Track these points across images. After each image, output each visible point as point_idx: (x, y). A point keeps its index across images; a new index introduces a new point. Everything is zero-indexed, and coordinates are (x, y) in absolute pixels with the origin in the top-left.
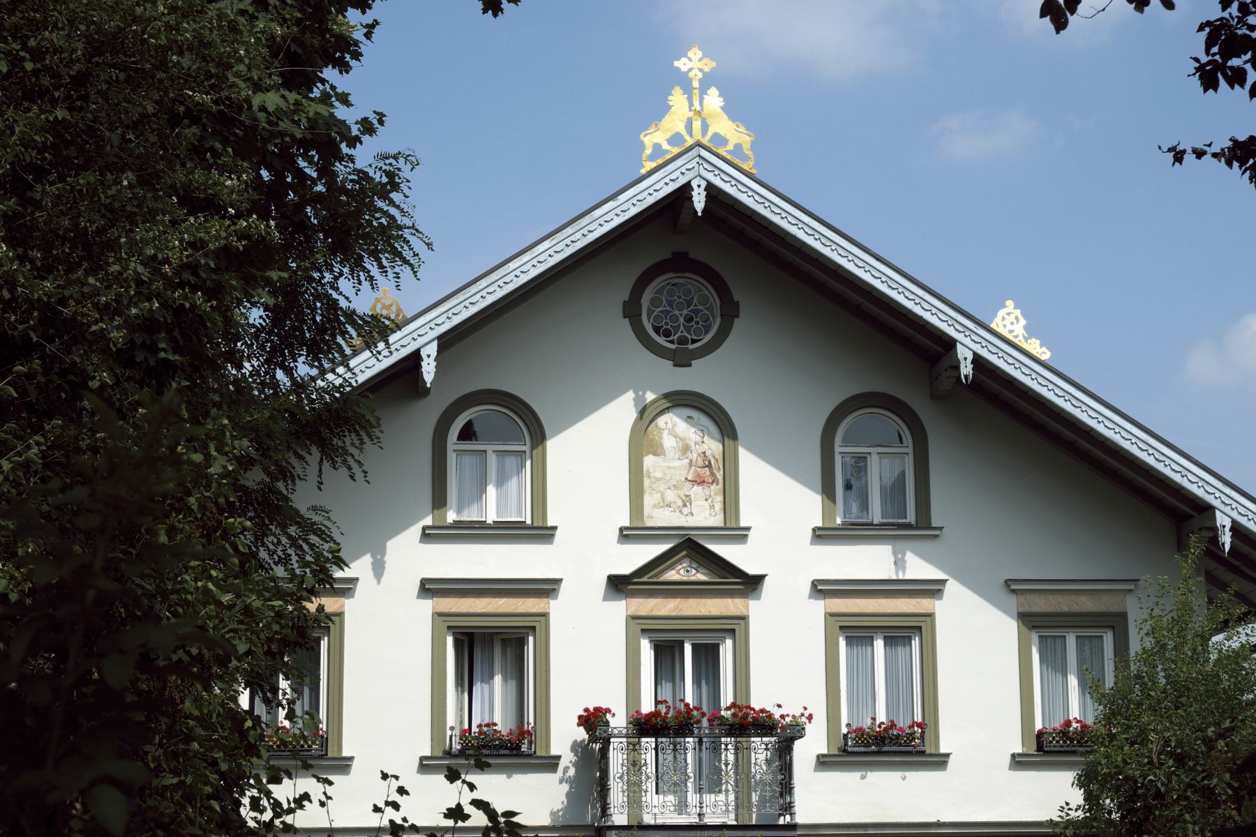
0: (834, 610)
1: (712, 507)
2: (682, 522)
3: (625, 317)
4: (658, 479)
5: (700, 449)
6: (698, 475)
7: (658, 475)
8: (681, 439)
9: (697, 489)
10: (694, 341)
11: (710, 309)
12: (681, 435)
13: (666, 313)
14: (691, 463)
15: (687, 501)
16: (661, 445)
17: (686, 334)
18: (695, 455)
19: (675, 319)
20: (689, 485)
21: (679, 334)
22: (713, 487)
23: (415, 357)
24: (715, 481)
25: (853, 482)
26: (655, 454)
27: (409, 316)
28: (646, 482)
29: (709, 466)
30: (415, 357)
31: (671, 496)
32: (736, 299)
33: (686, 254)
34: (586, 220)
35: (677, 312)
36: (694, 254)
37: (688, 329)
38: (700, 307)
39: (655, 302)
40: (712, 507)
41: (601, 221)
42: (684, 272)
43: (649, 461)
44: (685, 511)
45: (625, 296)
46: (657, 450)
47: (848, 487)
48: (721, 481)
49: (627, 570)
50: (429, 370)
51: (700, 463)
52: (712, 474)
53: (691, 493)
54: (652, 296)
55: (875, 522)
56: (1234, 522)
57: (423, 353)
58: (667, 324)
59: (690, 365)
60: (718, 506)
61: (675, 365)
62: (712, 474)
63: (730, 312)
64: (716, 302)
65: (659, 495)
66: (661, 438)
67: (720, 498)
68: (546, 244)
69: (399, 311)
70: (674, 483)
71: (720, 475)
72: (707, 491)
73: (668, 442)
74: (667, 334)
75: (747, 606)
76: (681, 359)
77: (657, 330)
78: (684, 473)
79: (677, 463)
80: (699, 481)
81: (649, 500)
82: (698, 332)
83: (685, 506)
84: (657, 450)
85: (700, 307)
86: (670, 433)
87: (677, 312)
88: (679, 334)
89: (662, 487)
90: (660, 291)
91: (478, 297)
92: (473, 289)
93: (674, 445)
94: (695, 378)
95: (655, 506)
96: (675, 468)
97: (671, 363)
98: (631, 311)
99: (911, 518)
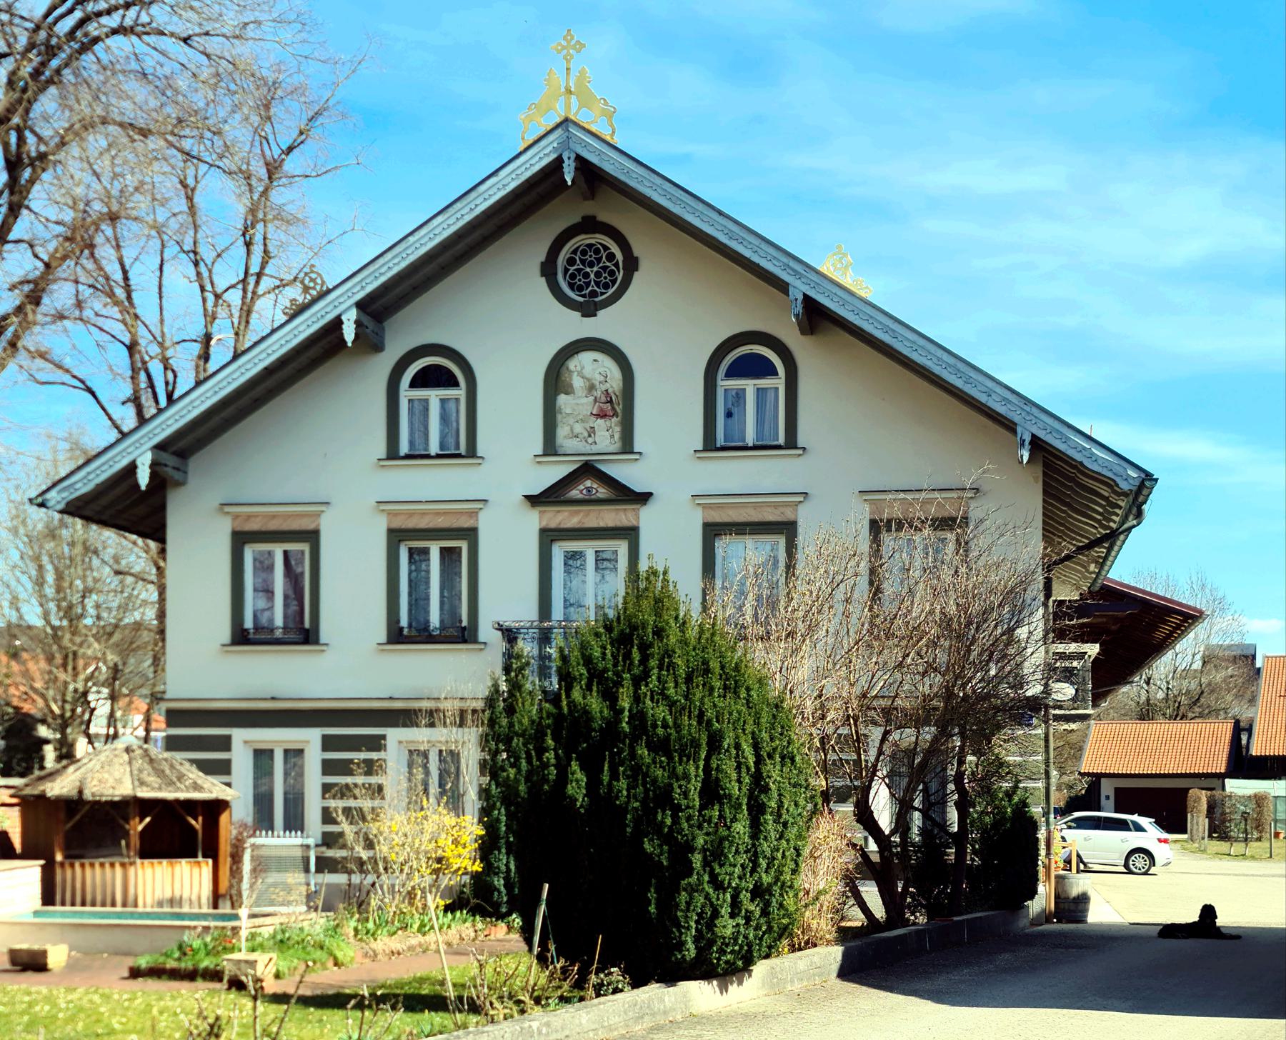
0: (710, 520)
1: (612, 436)
2: (588, 449)
3: (542, 276)
4: (568, 414)
5: (603, 387)
6: (601, 410)
7: (568, 411)
8: (588, 380)
9: (600, 421)
10: (602, 294)
11: (617, 265)
12: (588, 376)
13: (579, 270)
14: (595, 400)
15: (592, 432)
16: (571, 386)
17: (596, 288)
18: (599, 393)
19: (586, 275)
20: (593, 418)
21: (590, 288)
22: (614, 420)
23: (337, 323)
24: (615, 414)
25: (735, 410)
26: (567, 393)
27: (331, 287)
28: (559, 417)
29: (611, 401)
30: (337, 323)
31: (578, 428)
32: (636, 254)
33: (594, 217)
34: (473, 195)
35: (588, 270)
36: (604, 217)
37: (597, 284)
38: (608, 264)
39: (571, 261)
40: (612, 436)
41: (486, 196)
42: (594, 232)
43: (562, 399)
44: (590, 440)
45: (542, 258)
46: (569, 390)
47: (729, 415)
48: (620, 414)
49: (536, 492)
50: (349, 333)
51: (603, 399)
52: (613, 409)
53: (595, 425)
54: (568, 256)
55: (750, 444)
56: (1033, 436)
57: (344, 318)
58: (580, 280)
59: (595, 315)
60: (617, 436)
61: (583, 316)
62: (613, 409)
63: (632, 264)
64: (619, 256)
65: (569, 428)
66: (571, 379)
67: (618, 429)
68: (440, 219)
69: (323, 283)
70: (581, 417)
71: (619, 409)
72: (608, 423)
73: (577, 383)
74: (580, 289)
75: (638, 518)
76: (589, 309)
77: (571, 286)
78: (590, 409)
79: (585, 400)
80: (602, 415)
81: (562, 432)
82: (606, 286)
83: (590, 436)
84: (569, 390)
85: (608, 264)
86: (578, 375)
87: (588, 270)
88: (590, 288)
89: (571, 421)
90: (575, 252)
91: (385, 268)
92: (381, 261)
93: (582, 385)
94: (603, 325)
95: (565, 437)
96: (582, 404)
97: (578, 314)
98: (548, 271)
99: (781, 441)
